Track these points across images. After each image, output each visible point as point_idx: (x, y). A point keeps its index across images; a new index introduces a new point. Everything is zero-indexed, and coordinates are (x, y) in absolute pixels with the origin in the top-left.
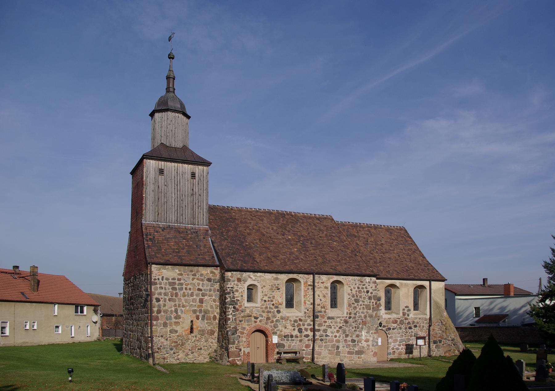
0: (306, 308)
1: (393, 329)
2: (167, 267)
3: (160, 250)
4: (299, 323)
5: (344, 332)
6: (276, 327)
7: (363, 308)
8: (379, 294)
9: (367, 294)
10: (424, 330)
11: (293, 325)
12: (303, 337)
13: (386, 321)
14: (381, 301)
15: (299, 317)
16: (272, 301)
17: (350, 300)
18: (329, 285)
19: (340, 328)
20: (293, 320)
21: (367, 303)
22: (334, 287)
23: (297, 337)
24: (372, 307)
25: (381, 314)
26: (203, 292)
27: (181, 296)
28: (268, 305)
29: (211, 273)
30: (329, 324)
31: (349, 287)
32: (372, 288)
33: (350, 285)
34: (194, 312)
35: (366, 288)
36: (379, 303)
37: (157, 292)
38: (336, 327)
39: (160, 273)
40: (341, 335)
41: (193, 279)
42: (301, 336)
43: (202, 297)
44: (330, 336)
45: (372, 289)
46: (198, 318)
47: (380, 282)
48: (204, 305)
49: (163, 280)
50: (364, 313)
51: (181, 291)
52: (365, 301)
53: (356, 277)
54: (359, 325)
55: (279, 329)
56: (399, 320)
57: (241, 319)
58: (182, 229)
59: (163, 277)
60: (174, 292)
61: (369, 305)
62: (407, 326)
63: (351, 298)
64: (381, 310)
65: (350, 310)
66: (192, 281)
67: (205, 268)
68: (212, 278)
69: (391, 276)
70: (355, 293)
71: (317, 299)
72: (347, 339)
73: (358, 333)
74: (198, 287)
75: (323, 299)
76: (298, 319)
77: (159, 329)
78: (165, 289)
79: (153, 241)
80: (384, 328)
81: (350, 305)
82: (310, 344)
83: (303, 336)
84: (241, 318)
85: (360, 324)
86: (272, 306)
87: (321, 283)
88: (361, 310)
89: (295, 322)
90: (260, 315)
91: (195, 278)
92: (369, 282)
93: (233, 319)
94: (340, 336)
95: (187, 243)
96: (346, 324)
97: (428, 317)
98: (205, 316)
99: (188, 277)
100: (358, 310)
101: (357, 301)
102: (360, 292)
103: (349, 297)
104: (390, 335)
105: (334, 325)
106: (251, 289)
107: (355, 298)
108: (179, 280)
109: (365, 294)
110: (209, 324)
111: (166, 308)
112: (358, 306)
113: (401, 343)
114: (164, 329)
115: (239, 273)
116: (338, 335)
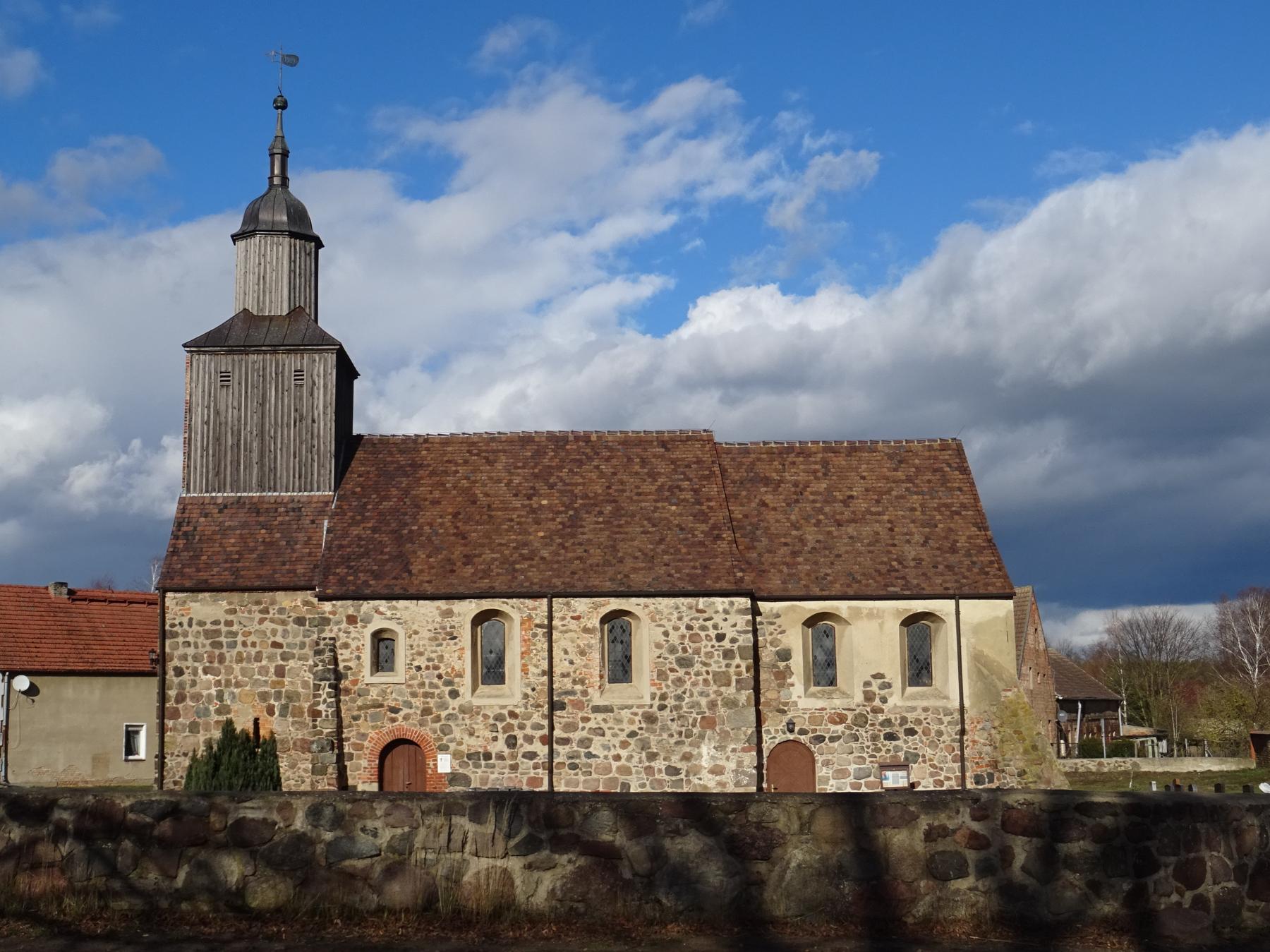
0: (528, 685)
1: (832, 739)
2: (201, 596)
3: (198, 557)
4: (509, 723)
5: (644, 745)
6: (447, 731)
7: (705, 681)
8: (783, 640)
9: (717, 644)
10: (944, 742)
11: (494, 728)
12: (520, 759)
13: (809, 718)
14: (791, 661)
15: (510, 708)
16: (436, 668)
17: (661, 660)
18: (595, 622)
19: (632, 734)
20: (492, 716)
21: (720, 667)
22: (622, 627)
23: (501, 757)
24: (734, 678)
25: (794, 698)
26: (285, 649)
27: (231, 662)
28: (427, 677)
29: (304, 605)
30: (597, 726)
31: (660, 626)
32: (735, 625)
33: (661, 623)
34: (264, 696)
35: (715, 627)
36: (787, 665)
37: (176, 653)
38: (618, 732)
39: (184, 610)
40: (634, 754)
41: (261, 621)
42: (514, 757)
43: (281, 662)
44: (599, 757)
45: (734, 629)
46: (271, 711)
47: (788, 608)
48: (287, 680)
49: (190, 625)
50: (708, 695)
51: (231, 650)
52: (712, 661)
53: (682, 600)
54: (690, 727)
55: (455, 738)
56: (850, 716)
57: (356, 713)
58: (267, 503)
59: (191, 620)
60: (217, 652)
61: (723, 672)
62: (880, 731)
63: (667, 655)
64: (792, 685)
65: (663, 685)
66: (260, 624)
67: (290, 593)
68: (308, 616)
69: (822, 590)
70: (677, 642)
71: (561, 660)
72: (653, 764)
73: (687, 749)
74: (272, 639)
75: (578, 661)
76: (505, 712)
77: (179, 739)
78: (196, 647)
79: (190, 537)
80: (802, 737)
81: (662, 675)
82: (541, 776)
83: (520, 755)
84: (358, 710)
85: (694, 725)
86: (436, 680)
87: (573, 618)
88: (700, 687)
89: (496, 720)
90: (405, 702)
91: (266, 619)
92: (726, 612)
93: (329, 713)
94: (630, 758)
95: (267, 536)
96: (650, 726)
97: (957, 704)
98: (288, 707)
99: (248, 616)
100: (688, 685)
101: (685, 663)
102: (694, 638)
103: (658, 652)
104: (824, 757)
105: (613, 729)
106: (381, 640)
107: (678, 655)
108: (229, 624)
109: (710, 644)
110: (297, 726)
111: (197, 689)
112: (687, 677)
113: (862, 781)
114: (192, 738)
115: (350, 602)
116: (624, 753)
